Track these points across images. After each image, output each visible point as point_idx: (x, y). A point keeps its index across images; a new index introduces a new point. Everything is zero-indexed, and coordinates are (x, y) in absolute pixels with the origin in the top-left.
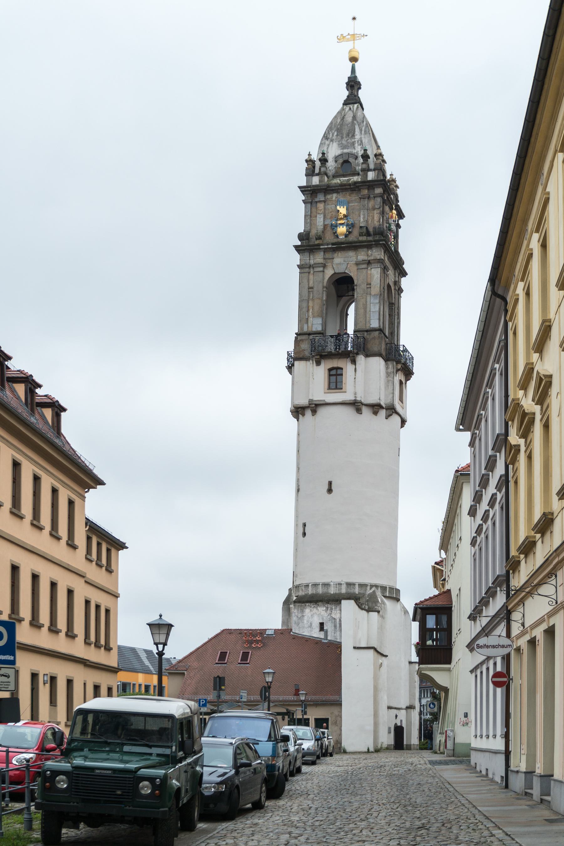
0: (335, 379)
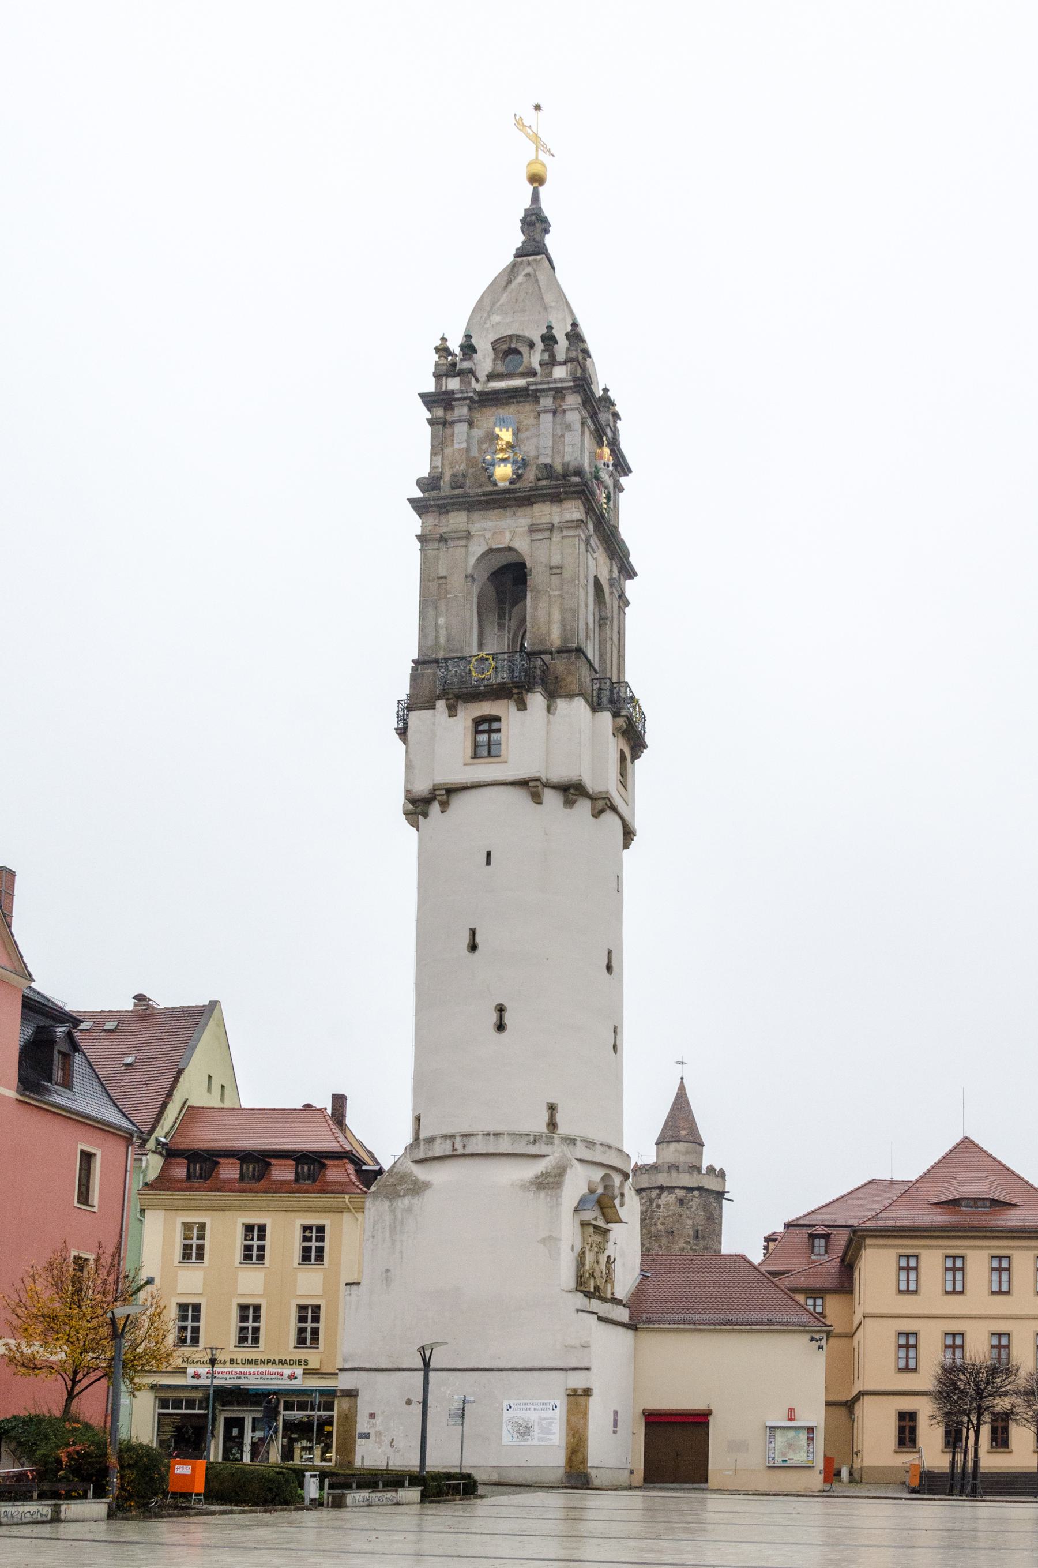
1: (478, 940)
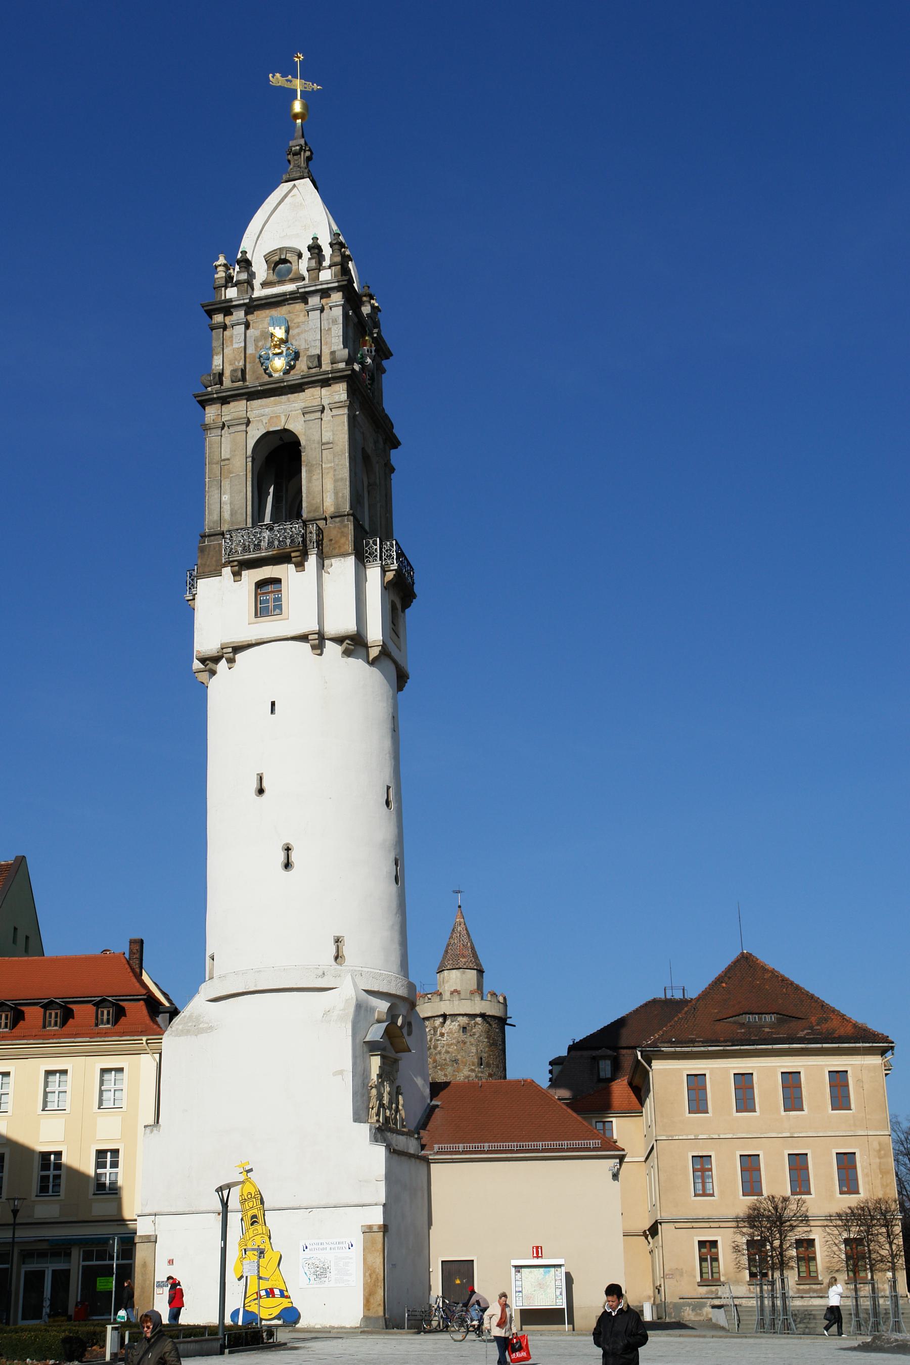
1: (265, 785)
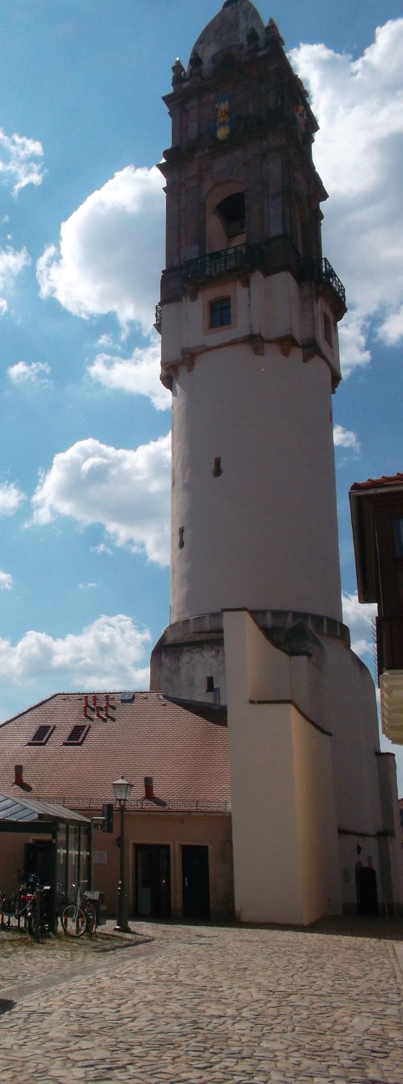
0: (220, 314)
1: (223, 467)
